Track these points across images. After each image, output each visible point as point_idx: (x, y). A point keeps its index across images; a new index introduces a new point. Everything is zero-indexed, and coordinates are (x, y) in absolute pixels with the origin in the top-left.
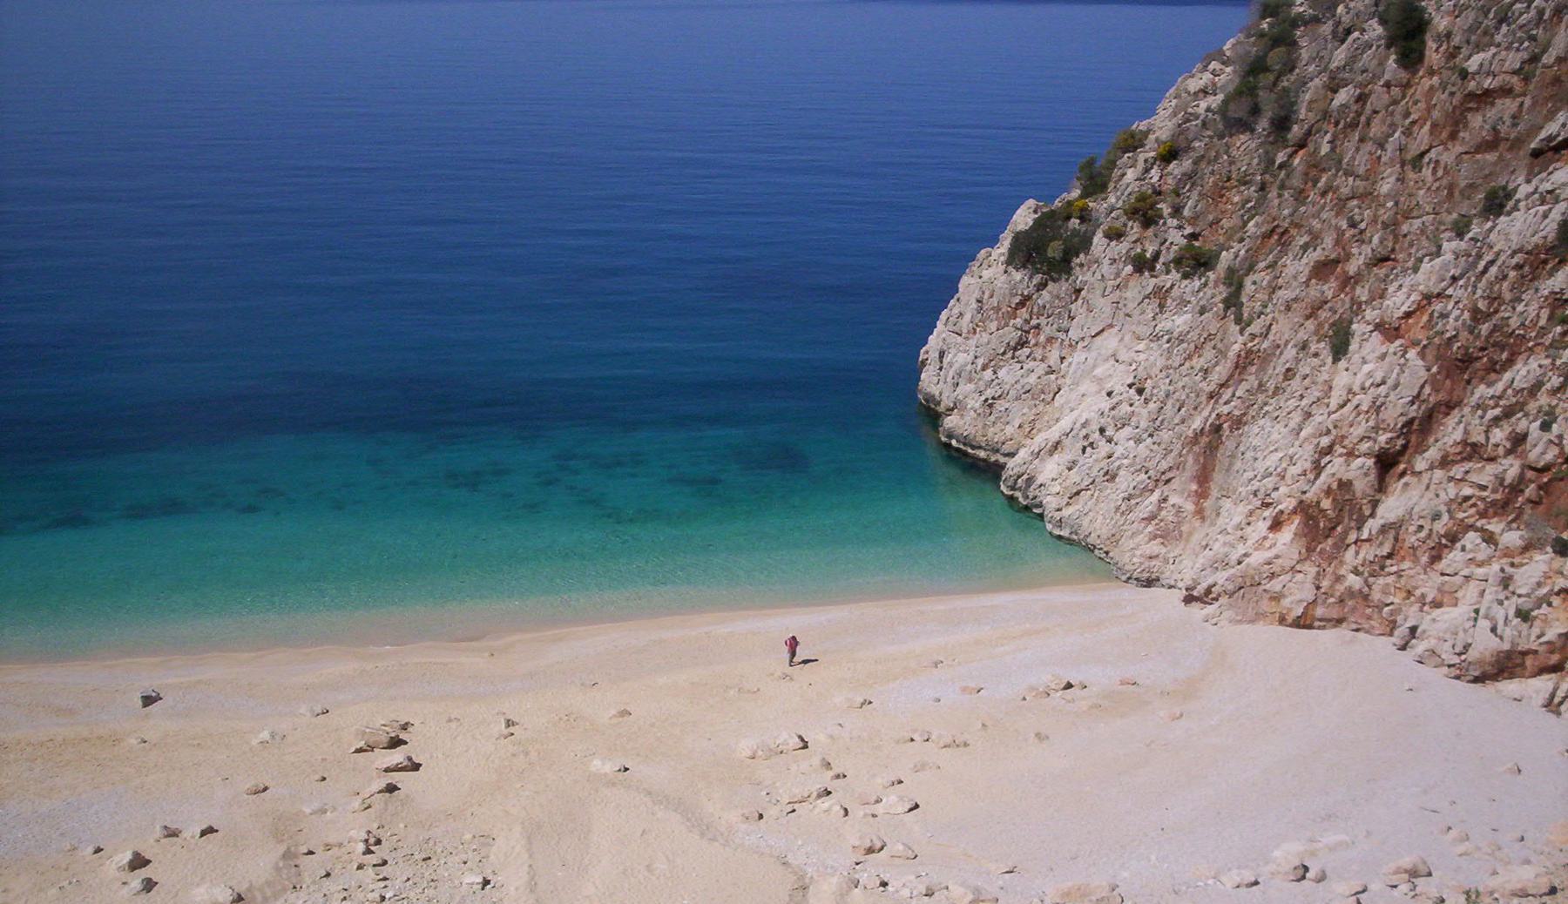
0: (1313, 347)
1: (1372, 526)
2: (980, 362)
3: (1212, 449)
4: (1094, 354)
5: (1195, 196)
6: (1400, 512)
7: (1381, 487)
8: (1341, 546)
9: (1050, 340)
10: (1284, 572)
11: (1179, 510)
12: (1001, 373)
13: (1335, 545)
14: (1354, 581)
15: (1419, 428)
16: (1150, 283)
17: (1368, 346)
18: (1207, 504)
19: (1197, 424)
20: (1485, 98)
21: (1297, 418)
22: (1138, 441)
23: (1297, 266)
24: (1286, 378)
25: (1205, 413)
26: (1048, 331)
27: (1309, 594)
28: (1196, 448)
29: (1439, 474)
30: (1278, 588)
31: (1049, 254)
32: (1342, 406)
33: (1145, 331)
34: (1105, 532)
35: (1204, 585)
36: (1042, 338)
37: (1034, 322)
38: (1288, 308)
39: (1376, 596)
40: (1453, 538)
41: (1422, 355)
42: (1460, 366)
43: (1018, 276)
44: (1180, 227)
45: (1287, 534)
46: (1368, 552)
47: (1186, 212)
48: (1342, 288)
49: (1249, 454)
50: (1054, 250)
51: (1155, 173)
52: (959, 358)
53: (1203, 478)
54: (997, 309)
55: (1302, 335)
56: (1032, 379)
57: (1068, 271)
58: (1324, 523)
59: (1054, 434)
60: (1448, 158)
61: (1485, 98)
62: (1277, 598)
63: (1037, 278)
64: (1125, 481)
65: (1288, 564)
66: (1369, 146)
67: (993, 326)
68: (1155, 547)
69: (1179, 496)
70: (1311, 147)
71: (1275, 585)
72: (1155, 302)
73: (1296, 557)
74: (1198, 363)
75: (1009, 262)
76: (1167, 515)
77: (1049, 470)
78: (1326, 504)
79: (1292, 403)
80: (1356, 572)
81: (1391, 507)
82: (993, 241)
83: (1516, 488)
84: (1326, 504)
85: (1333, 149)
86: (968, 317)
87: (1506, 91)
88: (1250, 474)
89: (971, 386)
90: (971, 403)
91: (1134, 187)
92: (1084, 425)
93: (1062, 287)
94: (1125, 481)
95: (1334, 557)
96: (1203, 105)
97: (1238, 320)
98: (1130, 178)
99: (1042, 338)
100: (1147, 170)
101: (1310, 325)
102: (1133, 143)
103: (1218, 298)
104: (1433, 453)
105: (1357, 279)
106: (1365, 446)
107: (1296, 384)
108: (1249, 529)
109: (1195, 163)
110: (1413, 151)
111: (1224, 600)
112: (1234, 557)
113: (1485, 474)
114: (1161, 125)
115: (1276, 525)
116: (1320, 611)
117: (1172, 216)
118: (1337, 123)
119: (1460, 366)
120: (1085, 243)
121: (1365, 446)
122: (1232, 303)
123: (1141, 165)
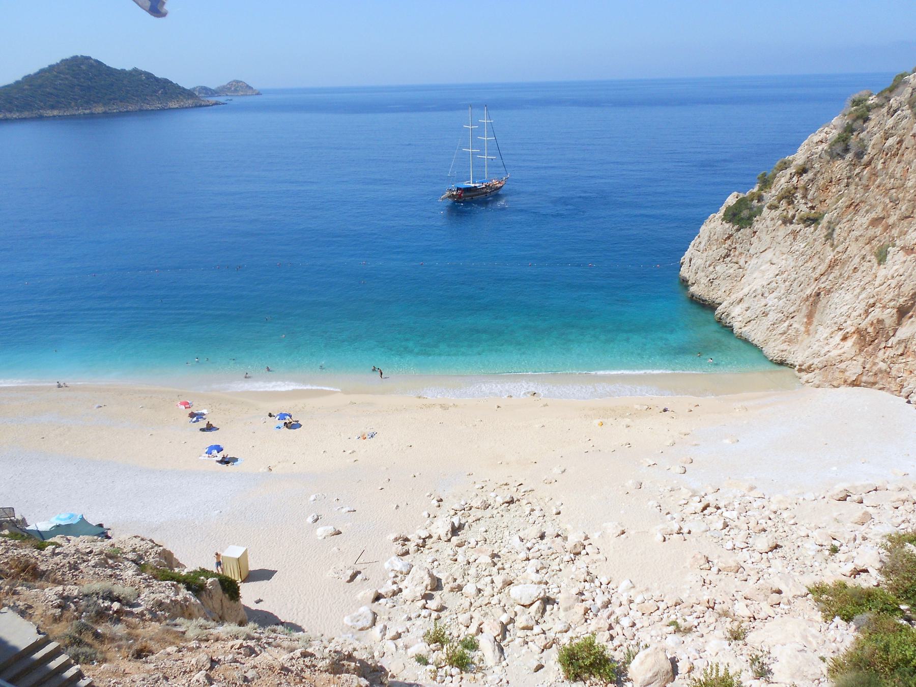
0: (868, 258)
1: (893, 341)
2: (708, 263)
3: (814, 304)
4: (761, 260)
5: (814, 190)
6: (909, 335)
7: (899, 323)
9: (741, 254)
10: (847, 360)
12: (717, 268)
13: (874, 349)
14: (883, 366)
16: (791, 227)
17: (896, 257)
18: (812, 328)
19: (808, 292)
21: (858, 290)
22: (780, 299)
23: (862, 220)
24: (854, 272)
25: (813, 287)
26: (739, 250)
27: (859, 370)
28: (807, 303)
30: (844, 367)
31: (741, 217)
32: (881, 285)
33: (786, 250)
34: (761, 339)
35: (808, 364)
36: (737, 253)
37: (733, 246)
38: (857, 240)
39: (894, 373)
43: (727, 226)
44: (806, 204)
46: (891, 352)
47: (809, 197)
48: (885, 230)
49: (833, 306)
50: (745, 213)
51: (795, 179)
52: (698, 262)
53: (810, 316)
54: (717, 240)
55: (863, 252)
56: (731, 271)
57: (751, 224)
58: (869, 339)
59: (740, 295)
62: (843, 372)
63: (736, 227)
64: (772, 316)
65: (849, 356)
66: (902, 164)
67: (715, 248)
68: (785, 346)
69: (798, 324)
70: (873, 165)
71: (843, 366)
72: (792, 237)
73: (854, 353)
74: (810, 265)
75: (723, 220)
76: (791, 332)
77: (736, 311)
78: (870, 330)
79: (856, 283)
80: (883, 361)
81: (904, 332)
82: (717, 211)
85: (884, 168)
86: (703, 244)
88: (833, 315)
89: (703, 274)
90: (702, 281)
91: (784, 186)
92: (754, 291)
93: (747, 231)
94: (772, 316)
96: (820, 148)
97: (832, 245)
98: (782, 182)
99: (737, 253)
100: (791, 178)
101: (868, 247)
102: (785, 166)
103: (822, 235)
105: (893, 226)
106: (892, 304)
107: (859, 274)
108: (831, 340)
109: (815, 175)
111: (817, 371)
112: (823, 352)
114: (799, 157)
115: (845, 338)
116: (864, 378)
117: (802, 198)
118: (887, 154)
120: (760, 211)
121: (892, 304)
122: (829, 236)
123: (788, 176)
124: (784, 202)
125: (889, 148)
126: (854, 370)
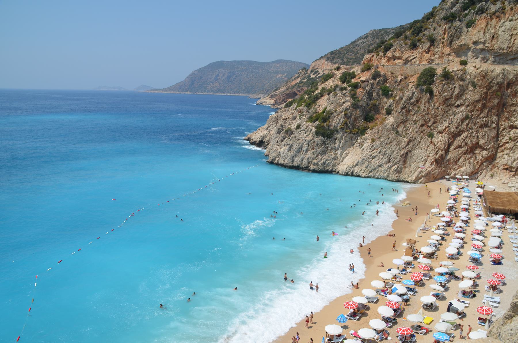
1: (445, 161)
7: (445, 155)
8: (441, 164)
15: (450, 145)
19: (402, 153)
40: (459, 159)
53: (405, 162)
54: (317, 145)
60: (444, 107)
68: (397, 175)
95: (441, 166)
105: (431, 126)
110: (436, 107)
119: (455, 136)
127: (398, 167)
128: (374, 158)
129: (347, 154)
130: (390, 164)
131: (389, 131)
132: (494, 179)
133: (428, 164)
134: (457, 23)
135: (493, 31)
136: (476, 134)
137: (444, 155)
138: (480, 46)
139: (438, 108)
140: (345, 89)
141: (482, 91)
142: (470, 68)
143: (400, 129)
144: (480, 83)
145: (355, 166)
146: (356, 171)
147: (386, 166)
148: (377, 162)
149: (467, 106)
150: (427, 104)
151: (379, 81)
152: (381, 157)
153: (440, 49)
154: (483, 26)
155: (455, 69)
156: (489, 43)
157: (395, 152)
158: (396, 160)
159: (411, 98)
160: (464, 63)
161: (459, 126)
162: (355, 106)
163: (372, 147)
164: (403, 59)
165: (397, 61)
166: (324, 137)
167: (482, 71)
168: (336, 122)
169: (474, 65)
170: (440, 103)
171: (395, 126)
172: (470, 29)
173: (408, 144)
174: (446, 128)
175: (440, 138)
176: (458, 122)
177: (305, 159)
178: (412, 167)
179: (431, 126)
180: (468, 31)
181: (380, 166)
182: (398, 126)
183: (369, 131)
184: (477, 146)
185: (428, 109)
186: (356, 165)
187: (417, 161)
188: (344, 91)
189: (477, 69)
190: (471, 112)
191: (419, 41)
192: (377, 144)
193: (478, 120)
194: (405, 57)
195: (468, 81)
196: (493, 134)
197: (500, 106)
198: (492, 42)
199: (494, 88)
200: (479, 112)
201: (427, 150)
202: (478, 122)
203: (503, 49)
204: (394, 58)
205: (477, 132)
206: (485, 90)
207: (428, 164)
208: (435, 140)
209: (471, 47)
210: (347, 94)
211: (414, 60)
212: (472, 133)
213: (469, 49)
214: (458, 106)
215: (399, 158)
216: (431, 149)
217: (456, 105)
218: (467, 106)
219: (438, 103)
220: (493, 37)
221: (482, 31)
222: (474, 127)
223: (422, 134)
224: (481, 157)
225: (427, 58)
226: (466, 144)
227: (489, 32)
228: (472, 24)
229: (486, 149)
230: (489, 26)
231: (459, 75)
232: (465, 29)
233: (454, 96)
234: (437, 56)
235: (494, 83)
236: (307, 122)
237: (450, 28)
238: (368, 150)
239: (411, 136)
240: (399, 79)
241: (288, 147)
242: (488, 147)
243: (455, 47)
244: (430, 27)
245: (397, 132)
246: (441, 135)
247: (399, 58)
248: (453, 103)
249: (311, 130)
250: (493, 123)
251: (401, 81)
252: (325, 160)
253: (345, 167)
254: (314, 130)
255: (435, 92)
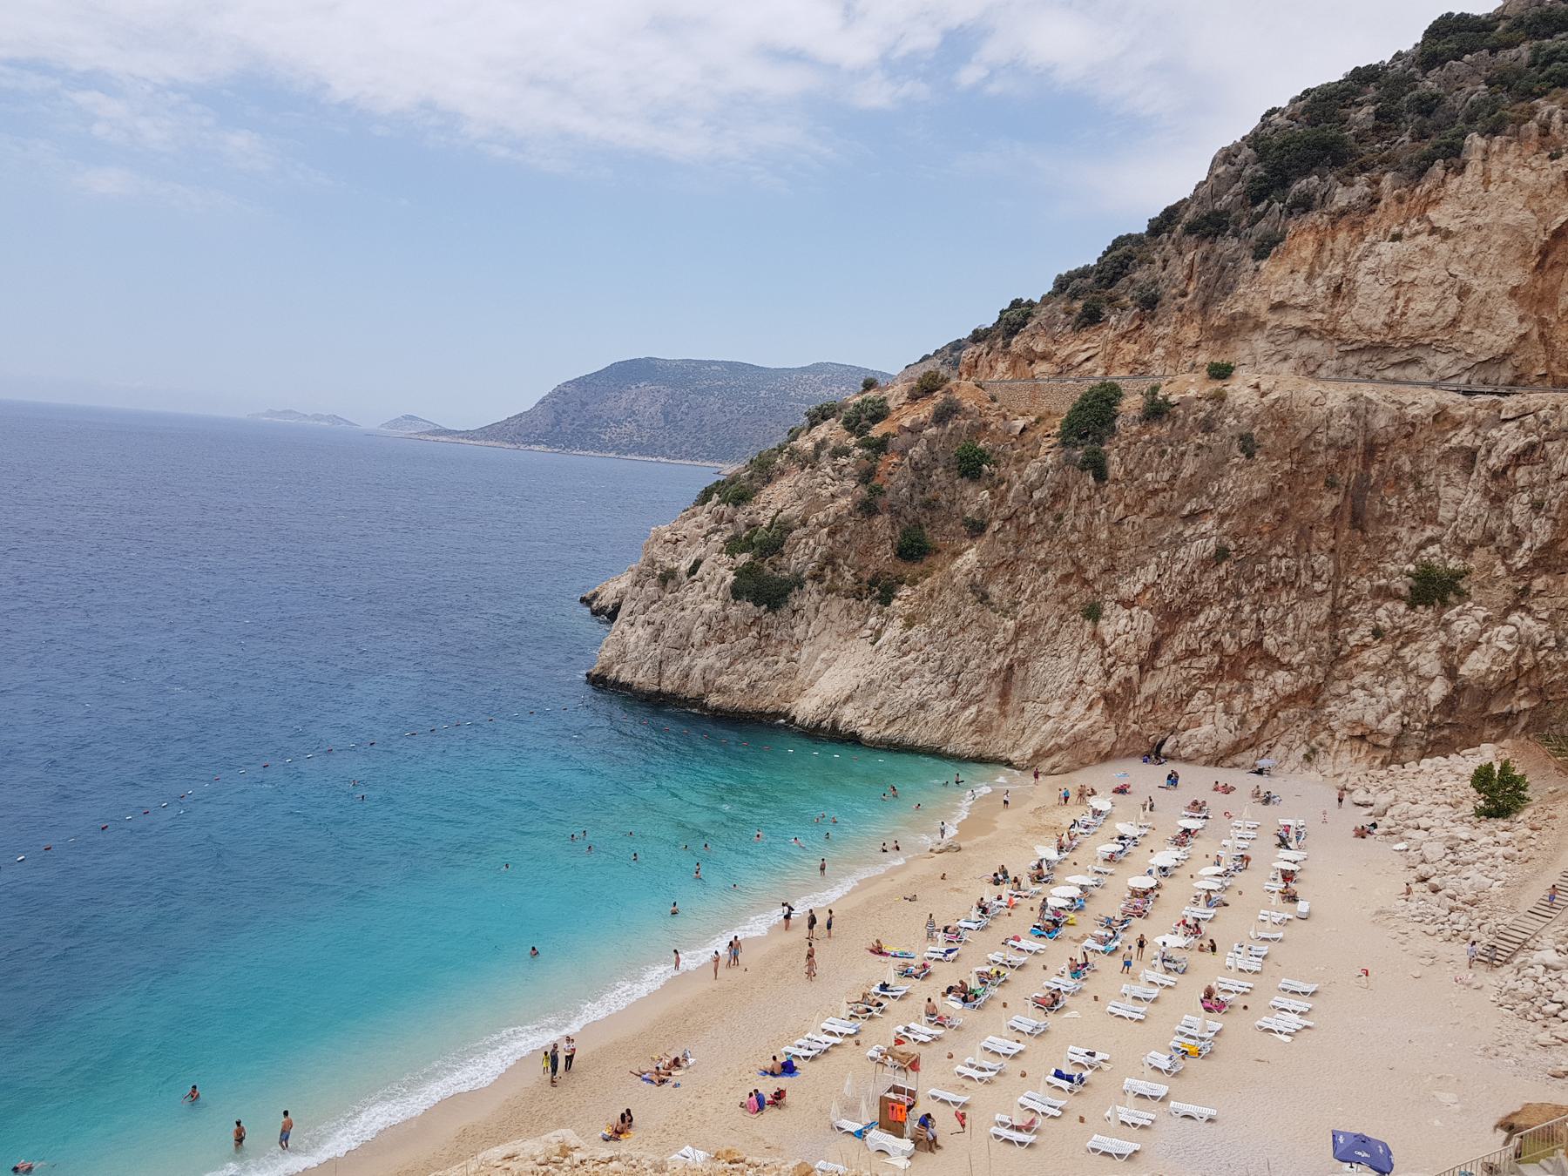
1: (1140, 699)
3: (1007, 680)
6: (1155, 688)
7: (1141, 681)
8: (1126, 710)
9: (781, 642)
11: (990, 714)
14: (1135, 727)
15: (1156, 648)
17: (1115, 613)
19: (995, 666)
20: (1155, 492)
21: (1075, 654)
29: (1174, 667)
39: (1145, 733)
40: (1190, 696)
41: (1151, 611)
42: (1172, 616)
45: (1098, 710)
53: (1004, 696)
54: (735, 628)
60: (1140, 520)
61: (1155, 492)
63: (764, 607)
68: (976, 738)
69: (990, 706)
78: (1119, 691)
81: (1149, 688)
83: (1220, 666)
84: (1119, 691)
87: (1164, 490)
93: (786, 611)
104: (1168, 657)
105: (1095, 580)
110: (1114, 518)
113: (1203, 663)
115: (1090, 708)
119: (1172, 616)
124: (828, 571)
125: (1041, 502)
126: (1108, 738)
127: (980, 711)
128: (904, 678)
129: (828, 663)
130: (954, 703)
131: (961, 594)
132: (1313, 774)
133: (1078, 708)
134: (1228, 245)
135: (1338, 271)
136: (1252, 612)
137: (1136, 679)
138: (1295, 320)
139: (1119, 522)
140: (846, 452)
141: (1274, 469)
142: (1239, 390)
143: (994, 590)
144: (1268, 443)
145: (846, 702)
146: (846, 719)
147: (940, 707)
148: (916, 693)
149: (1223, 518)
150: (1085, 508)
151: (956, 428)
152: (928, 677)
153: (1169, 330)
154: (1307, 252)
155: (1192, 392)
156: (1323, 311)
157: (972, 664)
158: (975, 691)
159: (1031, 489)
160: (1221, 372)
161: (1191, 583)
162: (867, 508)
163: (903, 642)
164: (1055, 359)
165: (1041, 368)
166: (757, 605)
167: (1277, 400)
168: (801, 556)
169: (1254, 381)
170: (1126, 505)
171: (979, 577)
172: (1264, 264)
173: (1015, 640)
174: (1146, 588)
175: (1123, 621)
176: (1187, 570)
177: (696, 672)
178: (1027, 715)
179: (1095, 580)
180: (1257, 269)
181: (922, 706)
182: (990, 577)
183: (905, 591)
184: (1257, 653)
185: (1089, 524)
186: (849, 698)
187: (1044, 697)
188: (842, 461)
189: (1263, 395)
190: (1236, 536)
191: (1111, 300)
192: (918, 633)
193: (1259, 567)
194: (1063, 353)
195: (1229, 434)
196: (1317, 611)
197: (1341, 519)
198: (1333, 306)
199: (1319, 461)
200: (1267, 538)
201: (1078, 660)
202: (1260, 574)
203: (1370, 332)
204: (1032, 358)
205: (1258, 606)
206: (1287, 467)
207: (1078, 708)
208: (1107, 629)
209: (1264, 323)
210: (849, 469)
211: (1089, 365)
212: (1238, 608)
213: (1259, 326)
214: (1193, 517)
215: (982, 683)
216: (1092, 657)
217: (1185, 513)
218: (1223, 518)
219: (1121, 506)
220: (1338, 289)
221: (1305, 269)
222: (1245, 590)
223: (1064, 608)
224: (1267, 693)
225: (1128, 359)
226: (1217, 645)
227: (1327, 273)
228: (1271, 247)
229: (1288, 667)
230: (1326, 254)
231: (1202, 414)
232: (1250, 264)
233: (1178, 483)
234: (1159, 351)
235: (1319, 443)
236: (720, 552)
237: (1206, 259)
238: (892, 652)
239: (1028, 611)
240: (1020, 423)
241: (650, 629)
242: (1295, 661)
243: (1215, 321)
244: (1156, 257)
245: (984, 598)
246: (1127, 612)
247: (1045, 357)
248: (1175, 505)
249: (723, 580)
250: (1316, 577)
251: (1024, 429)
252: (754, 677)
253: (816, 701)
254: (731, 578)
255: (1115, 469)
